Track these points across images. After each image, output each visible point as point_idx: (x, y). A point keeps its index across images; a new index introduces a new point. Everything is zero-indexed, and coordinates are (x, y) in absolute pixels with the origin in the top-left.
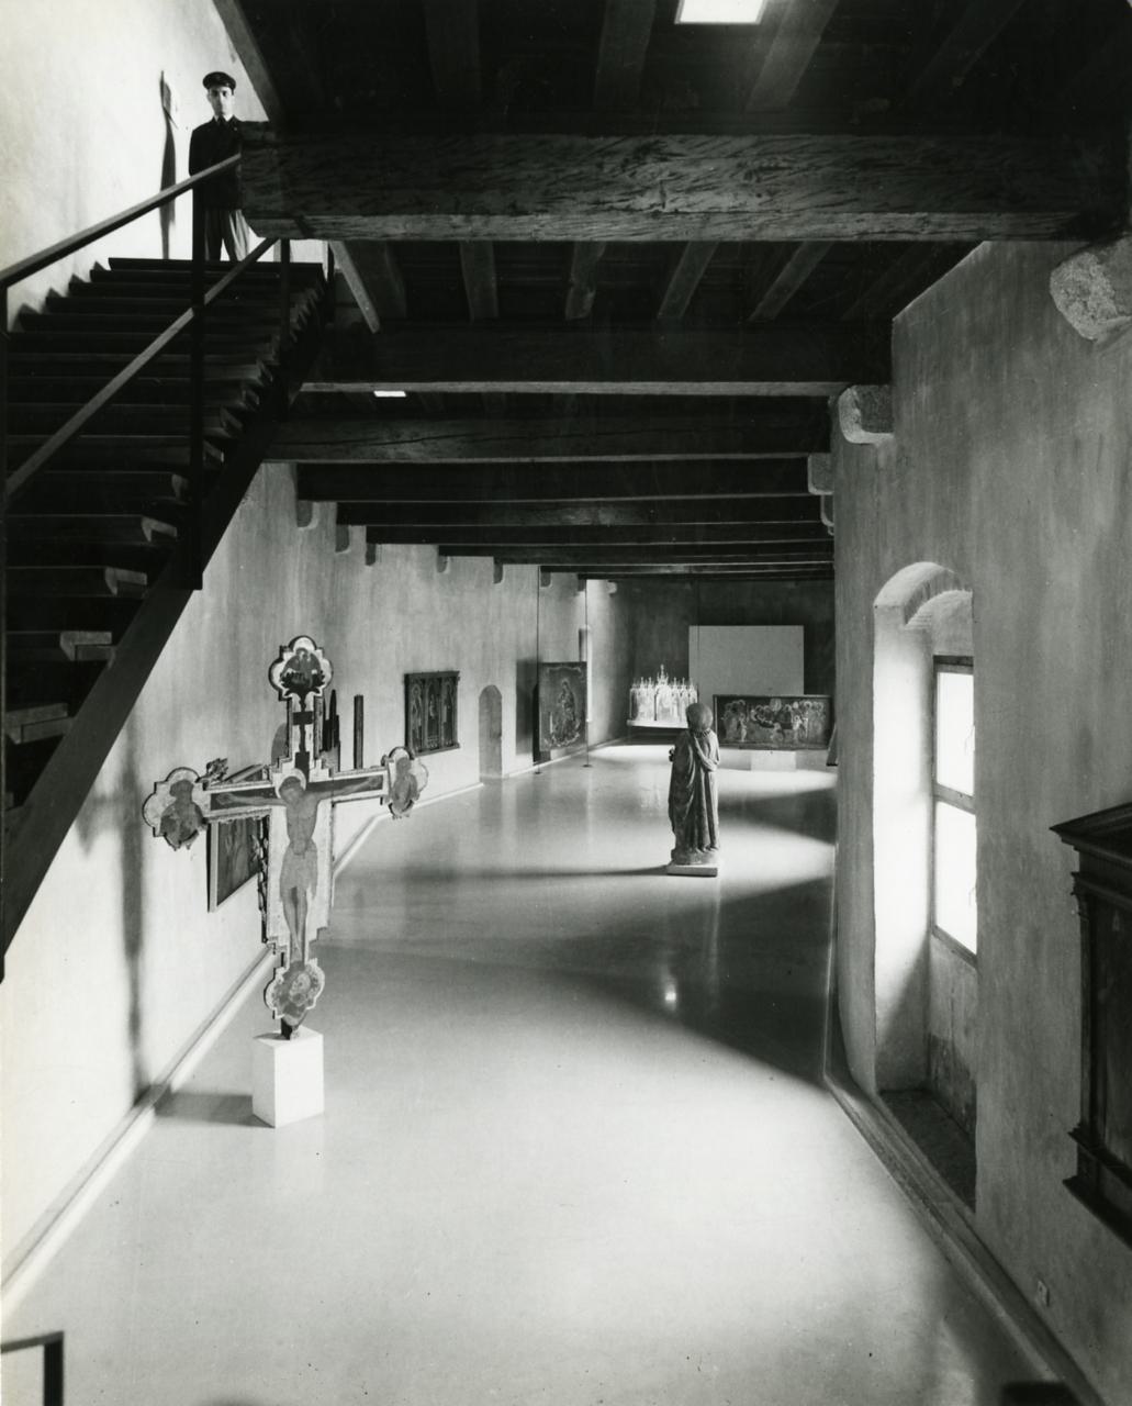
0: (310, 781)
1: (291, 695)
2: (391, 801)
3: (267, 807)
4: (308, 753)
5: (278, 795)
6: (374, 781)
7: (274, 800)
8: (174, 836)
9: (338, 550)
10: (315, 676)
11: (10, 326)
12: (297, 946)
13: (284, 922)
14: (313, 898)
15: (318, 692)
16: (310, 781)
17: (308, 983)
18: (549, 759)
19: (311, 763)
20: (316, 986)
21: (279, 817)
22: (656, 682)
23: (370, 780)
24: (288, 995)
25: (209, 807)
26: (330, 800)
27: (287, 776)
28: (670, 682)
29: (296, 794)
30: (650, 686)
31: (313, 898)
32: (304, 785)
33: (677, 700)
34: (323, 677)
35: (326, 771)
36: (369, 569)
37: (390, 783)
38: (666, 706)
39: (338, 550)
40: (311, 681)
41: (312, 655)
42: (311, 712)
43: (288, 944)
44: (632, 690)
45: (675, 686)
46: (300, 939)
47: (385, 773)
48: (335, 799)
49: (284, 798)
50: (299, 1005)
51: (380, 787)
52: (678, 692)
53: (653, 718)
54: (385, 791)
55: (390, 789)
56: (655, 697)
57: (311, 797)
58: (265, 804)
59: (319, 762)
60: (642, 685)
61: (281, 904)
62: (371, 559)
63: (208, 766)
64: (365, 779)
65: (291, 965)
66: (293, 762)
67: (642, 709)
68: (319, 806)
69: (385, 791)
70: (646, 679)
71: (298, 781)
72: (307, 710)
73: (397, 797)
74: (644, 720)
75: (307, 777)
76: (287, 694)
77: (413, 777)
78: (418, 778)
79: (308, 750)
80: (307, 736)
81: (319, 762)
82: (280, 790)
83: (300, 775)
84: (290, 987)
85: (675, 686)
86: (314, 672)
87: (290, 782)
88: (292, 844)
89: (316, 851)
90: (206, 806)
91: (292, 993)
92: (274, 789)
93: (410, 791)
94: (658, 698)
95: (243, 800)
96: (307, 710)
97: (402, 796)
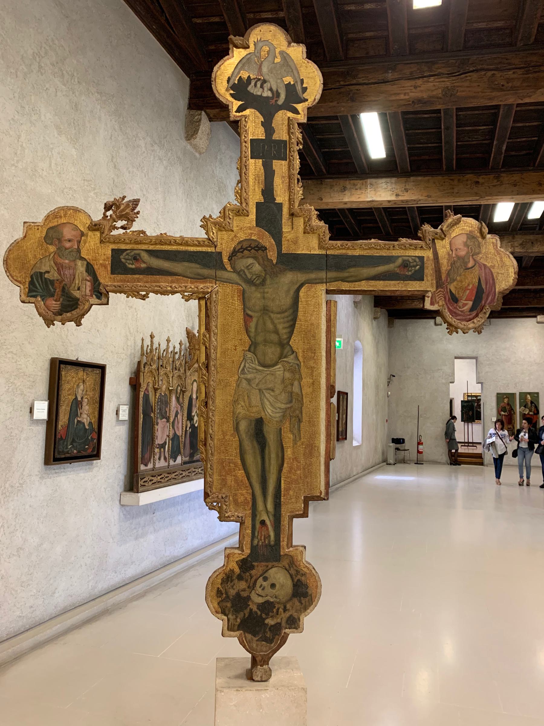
0: (284, 250)
1: (247, 112)
4: (280, 206)
5: (228, 267)
6: (405, 265)
7: (220, 273)
8: (54, 304)
10: (288, 86)
11: (244, 102)
16: (284, 250)
23: (400, 261)
24: (249, 598)
27: (242, 236)
29: (257, 268)
31: (295, 442)
32: (273, 255)
34: (305, 90)
40: (283, 96)
46: (270, 506)
49: (235, 271)
50: (270, 622)
63: (108, 207)
65: (253, 548)
66: (253, 216)
71: (264, 249)
72: (275, 137)
75: (279, 244)
76: (240, 109)
79: (278, 200)
83: (268, 241)
84: (252, 587)
86: (289, 79)
90: (104, 266)
91: (254, 596)
92: (220, 254)
95: (165, 265)
96: (275, 137)
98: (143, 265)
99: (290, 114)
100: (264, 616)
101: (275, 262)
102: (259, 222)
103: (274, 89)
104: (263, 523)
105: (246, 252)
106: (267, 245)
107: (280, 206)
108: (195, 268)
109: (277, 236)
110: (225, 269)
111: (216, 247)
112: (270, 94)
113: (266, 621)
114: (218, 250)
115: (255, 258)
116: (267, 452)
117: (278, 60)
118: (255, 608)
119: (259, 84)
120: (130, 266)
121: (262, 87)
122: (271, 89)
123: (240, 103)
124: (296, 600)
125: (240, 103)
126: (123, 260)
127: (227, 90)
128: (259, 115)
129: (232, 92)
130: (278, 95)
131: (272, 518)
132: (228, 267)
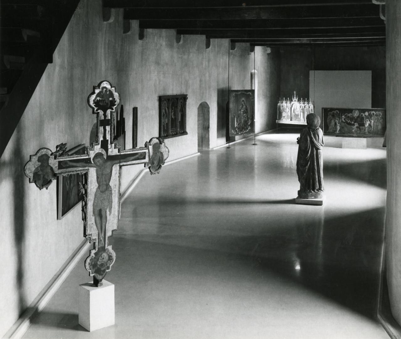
0: (109, 154)
2: (150, 165)
3: (87, 168)
4: (108, 140)
8: (41, 182)
9: (125, 32)
12: (102, 239)
13: (95, 227)
14: (110, 214)
15: (113, 109)
16: (109, 154)
17: (107, 258)
18: (234, 140)
19: (109, 146)
20: (111, 259)
21: (93, 173)
22: (291, 101)
24: (97, 263)
25: (57, 168)
26: (118, 165)
27: (97, 152)
28: (299, 100)
29: (101, 161)
30: (288, 102)
31: (110, 214)
32: (105, 157)
33: (303, 109)
34: (115, 101)
35: (117, 150)
36: (140, 42)
37: (149, 156)
38: (297, 113)
39: (125, 32)
40: (109, 104)
41: (110, 90)
42: (109, 120)
43: (97, 238)
44: (279, 104)
45: (302, 102)
46: (103, 234)
47: (147, 151)
48: (121, 164)
50: (102, 269)
51: (144, 158)
52: (303, 105)
53: (290, 119)
54: (147, 160)
55: (149, 159)
56: (291, 108)
57: (109, 163)
58: (85, 167)
59: (113, 145)
60: (284, 102)
61: (93, 218)
62: (141, 37)
63: (57, 147)
64: (137, 154)
65: (99, 248)
67: (284, 114)
68: (113, 168)
69: (147, 160)
70: (286, 99)
71: (103, 155)
73: (153, 163)
74: (285, 120)
76: (97, 110)
77: (162, 153)
78: (163, 154)
80: (107, 132)
81: (113, 145)
82: (93, 160)
83: (104, 152)
84: (98, 260)
85: (302, 102)
86: (111, 99)
87: (98, 155)
88: (99, 187)
89: (111, 191)
90: (56, 167)
91: (99, 263)
92: (90, 158)
93: (160, 160)
94: (292, 109)
95: (74, 164)
97: (156, 163)
98: (68, 165)
99: (111, 110)
100: (101, 268)
101: (106, 159)
102: (102, 147)
103: (107, 102)
104: (101, 240)
105: (98, 157)
106: (103, 153)
107: (108, 140)
108: (84, 164)
109: (107, 150)
110: (91, 163)
111: (89, 156)
112: (106, 104)
113: (102, 269)
114: (90, 157)
115: (100, 158)
116: (102, 219)
117: (108, 93)
118: (99, 266)
119: (102, 102)
120: (64, 166)
121: (103, 102)
122: (106, 103)
123: (97, 108)
124: (109, 261)
125: (97, 108)
126: (62, 165)
127: (93, 104)
128: (103, 112)
129: (94, 104)
130: (108, 104)
131: (103, 238)
132: (93, 162)
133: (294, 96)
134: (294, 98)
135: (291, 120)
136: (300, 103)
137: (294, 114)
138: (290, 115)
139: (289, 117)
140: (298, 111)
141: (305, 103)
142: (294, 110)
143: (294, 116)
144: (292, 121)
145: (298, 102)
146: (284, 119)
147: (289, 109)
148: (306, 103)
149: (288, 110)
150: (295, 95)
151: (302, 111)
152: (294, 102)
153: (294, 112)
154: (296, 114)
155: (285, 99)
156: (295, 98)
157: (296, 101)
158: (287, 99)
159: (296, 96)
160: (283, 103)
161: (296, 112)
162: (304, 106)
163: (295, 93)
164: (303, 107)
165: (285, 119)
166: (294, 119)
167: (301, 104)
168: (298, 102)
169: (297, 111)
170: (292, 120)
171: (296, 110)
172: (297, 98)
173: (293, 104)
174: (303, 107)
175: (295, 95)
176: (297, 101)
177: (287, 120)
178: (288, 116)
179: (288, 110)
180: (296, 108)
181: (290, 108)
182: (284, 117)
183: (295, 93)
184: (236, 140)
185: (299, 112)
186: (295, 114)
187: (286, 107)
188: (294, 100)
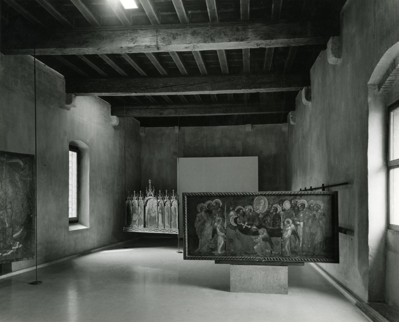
18: (11, 271)
22: (145, 195)
28: (156, 195)
30: (141, 198)
33: (162, 209)
38: (153, 215)
44: (127, 202)
45: (160, 197)
52: (162, 202)
53: (143, 225)
56: (145, 207)
60: (135, 198)
67: (135, 217)
70: (138, 194)
74: (138, 228)
85: (160, 197)
94: (147, 208)
133: (148, 188)
134: (148, 191)
135: (145, 227)
136: (158, 199)
137: (148, 216)
138: (143, 218)
139: (142, 222)
140: (155, 211)
141: (164, 199)
142: (149, 210)
143: (148, 219)
144: (146, 228)
145: (154, 196)
146: (135, 225)
147: (141, 208)
148: (167, 197)
149: (140, 210)
150: (150, 186)
151: (160, 211)
152: (150, 197)
153: (149, 213)
154: (151, 216)
155: (136, 193)
156: (150, 190)
157: (151, 195)
158: (139, 193)
159: (152, 188)
160: (132, 199)
161: (152, 214)
162: (163, 203)
163: (150, 183)
164: (161, 204)
165: (136, 225)
166: (149, 224)
167: (159, 200)
168: (154, 196)
169: (154, 212)
170: (146, 226)
171: (152, 210)
172: (153, 190)
173: (147, 201)
174: (161, 204)
175: (150, 186)
176: (153, 195)
177: (139, 226)
178: (140, 219)
179: (140, 210)
180: (153, 207)
181: (143, 207)
182: (134, 221)
183: (150, 183)
184: (13, 271)
185: (157, 212)
186: (151, 217)
187: (137, 207)
188: (148, 195)
